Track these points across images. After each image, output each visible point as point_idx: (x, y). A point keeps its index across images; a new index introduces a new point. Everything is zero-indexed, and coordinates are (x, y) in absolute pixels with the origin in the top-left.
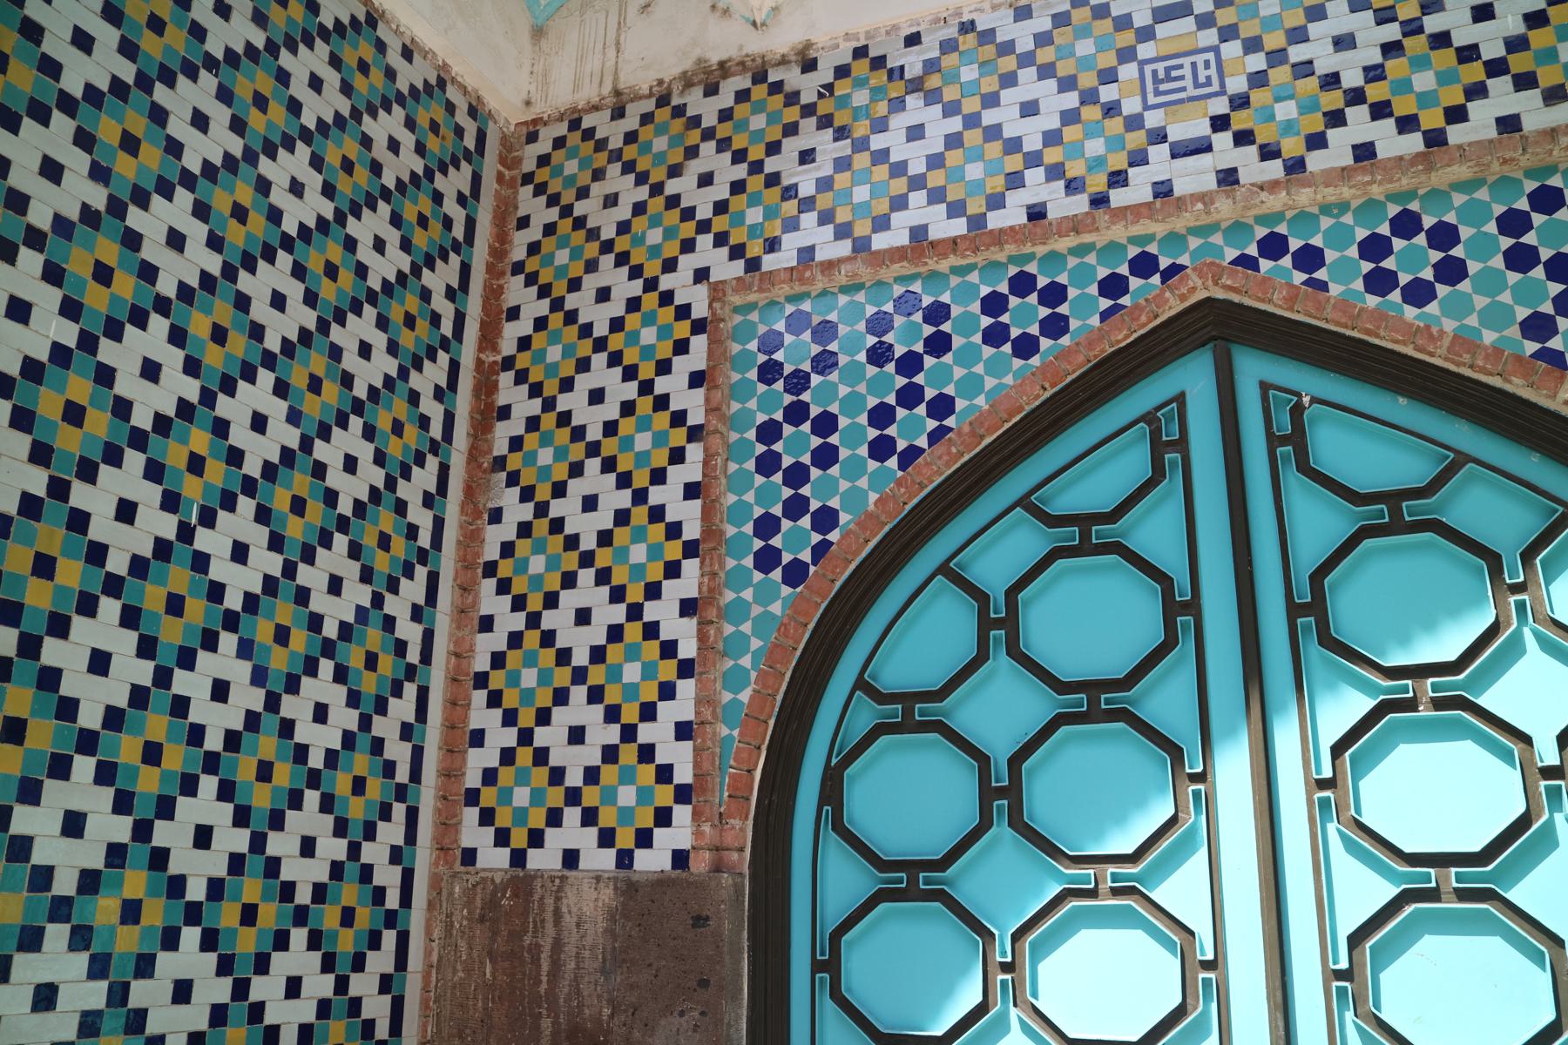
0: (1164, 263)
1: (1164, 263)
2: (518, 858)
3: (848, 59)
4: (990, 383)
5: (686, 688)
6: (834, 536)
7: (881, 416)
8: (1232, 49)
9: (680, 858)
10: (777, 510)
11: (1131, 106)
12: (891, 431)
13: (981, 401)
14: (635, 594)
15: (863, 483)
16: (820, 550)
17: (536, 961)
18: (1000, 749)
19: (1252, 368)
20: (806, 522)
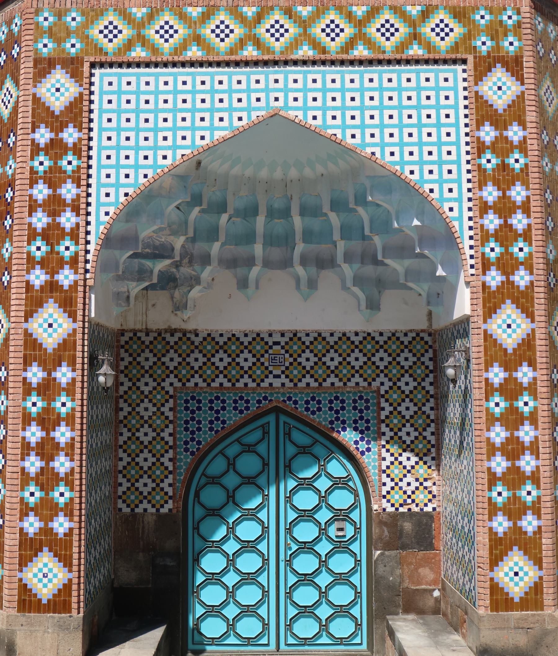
0: (269, 398)
1: (269, 398)
3: (206, 336)
4: (234, 418)
5: (171, 476)
7: (211, 422)
8: (287, 356)
10: (189, 440)
11: (266, 364)
12: (213, 426)
13: (232, 422)
14: (158, 456)
15: (207, 436)
16: (198, 449)
19: (283, 418)
20: (195, 443)
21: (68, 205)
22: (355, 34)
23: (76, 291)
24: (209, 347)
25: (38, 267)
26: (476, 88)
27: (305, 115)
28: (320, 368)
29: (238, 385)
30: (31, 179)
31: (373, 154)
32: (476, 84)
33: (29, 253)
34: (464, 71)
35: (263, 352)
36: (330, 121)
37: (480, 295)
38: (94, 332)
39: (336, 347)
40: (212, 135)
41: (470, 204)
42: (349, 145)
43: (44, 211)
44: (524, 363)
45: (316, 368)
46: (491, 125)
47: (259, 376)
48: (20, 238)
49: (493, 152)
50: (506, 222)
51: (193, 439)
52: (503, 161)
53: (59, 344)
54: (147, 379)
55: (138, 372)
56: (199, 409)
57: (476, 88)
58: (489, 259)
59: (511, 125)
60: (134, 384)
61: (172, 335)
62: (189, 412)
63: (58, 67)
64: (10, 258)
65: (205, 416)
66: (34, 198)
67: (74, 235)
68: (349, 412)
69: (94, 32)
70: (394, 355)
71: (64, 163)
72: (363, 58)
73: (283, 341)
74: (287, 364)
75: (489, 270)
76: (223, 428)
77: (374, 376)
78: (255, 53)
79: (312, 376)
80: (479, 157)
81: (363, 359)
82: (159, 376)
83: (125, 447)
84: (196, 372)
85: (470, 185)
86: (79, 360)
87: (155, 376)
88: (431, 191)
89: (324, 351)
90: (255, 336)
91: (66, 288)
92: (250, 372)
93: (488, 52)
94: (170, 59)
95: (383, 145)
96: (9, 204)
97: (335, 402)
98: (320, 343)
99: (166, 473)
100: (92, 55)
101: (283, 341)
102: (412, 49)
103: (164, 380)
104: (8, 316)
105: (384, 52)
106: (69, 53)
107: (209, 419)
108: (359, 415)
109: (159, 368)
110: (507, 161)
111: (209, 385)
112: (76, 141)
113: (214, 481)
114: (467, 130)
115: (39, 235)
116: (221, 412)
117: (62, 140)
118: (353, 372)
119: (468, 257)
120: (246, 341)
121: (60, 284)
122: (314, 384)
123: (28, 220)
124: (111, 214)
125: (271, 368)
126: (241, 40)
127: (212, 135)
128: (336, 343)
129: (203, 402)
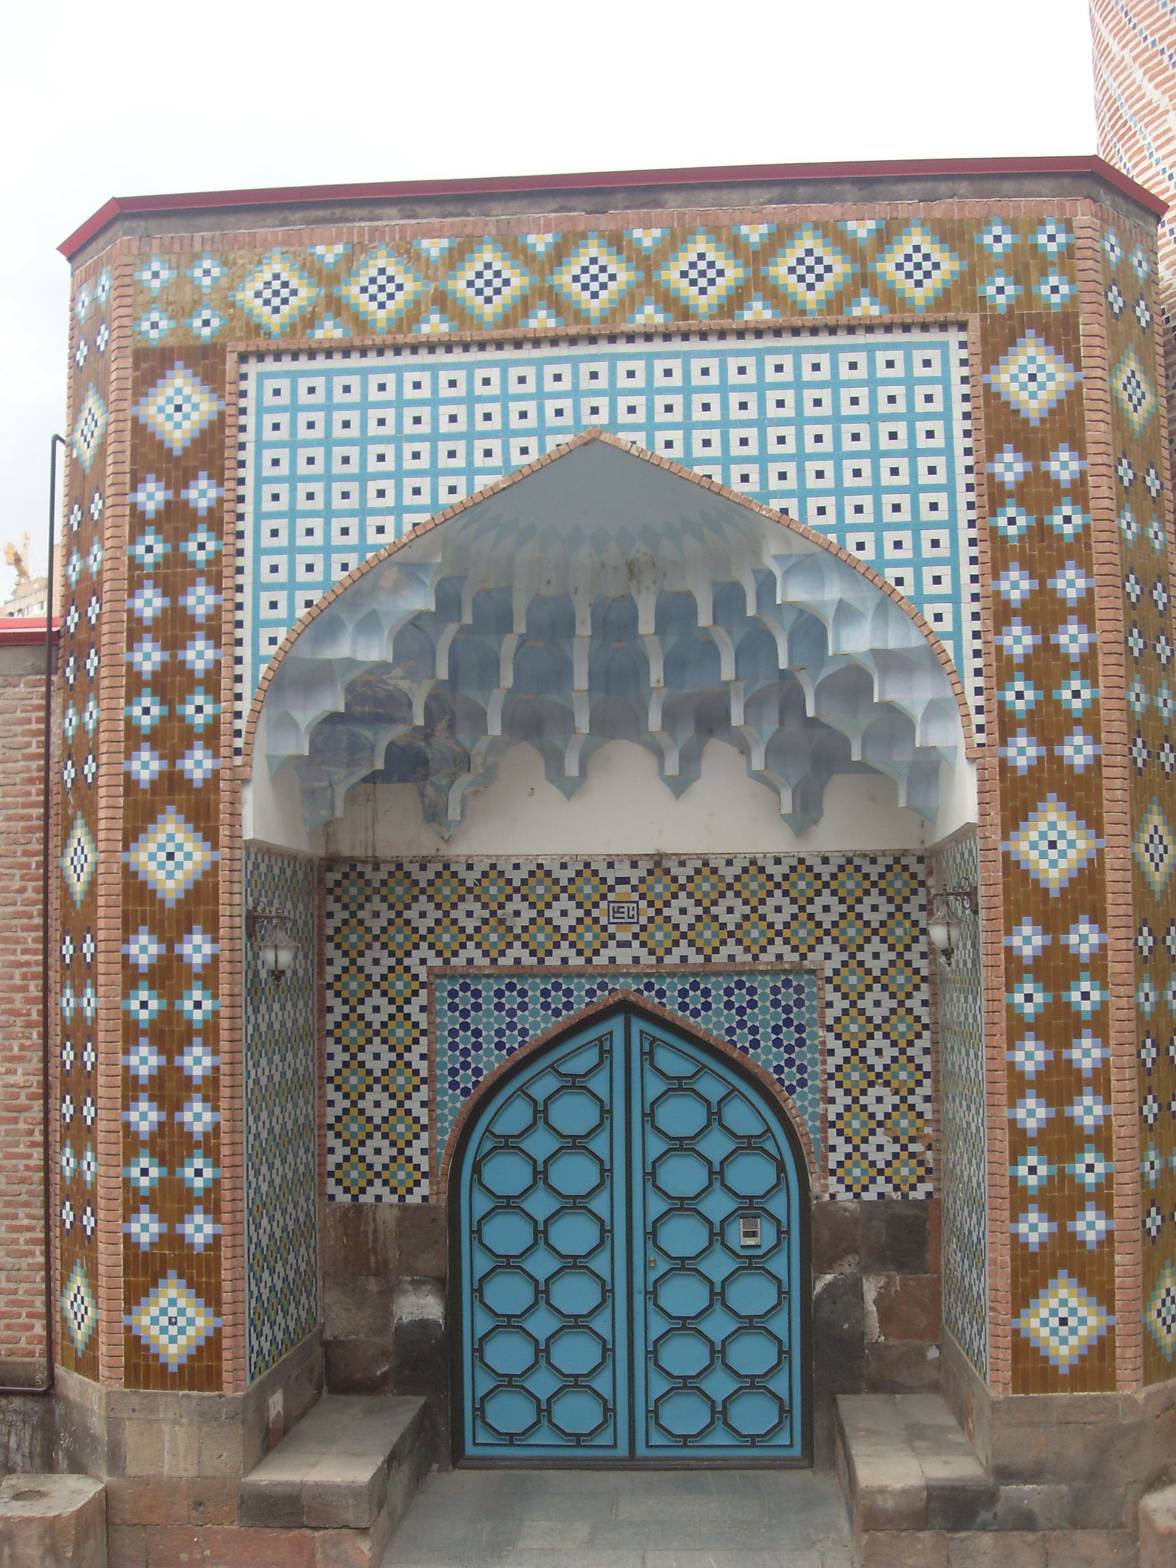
2: (355, 1198)
4: (543, 1025)
5: (425, 1135)
6: (481, 1079)
8: (643, 904)
9: (425, 1198)
10: (458, 1066)
16: (476, 1084)
17: (366, 1236)
18: (540, 1158)
19: (637, 1025)
20: (469, 1072)
21: (200, 627)
22: (747, 280)
23: (217, 790)
24: (493, 890)
25: (146, 745)
26: (985, 379)
27: (650, 441)
28: (707, 927)
29: (548, 961)
30: (131, 578)
31: (785, 511)
32: (986, 370)
33: (128, 720)
34: (963, 345)
35: (596, 898)
36: (698, 451)
37: (996, 784)
38: (256, 866)
39: (738, 886)
40: (470, 485)
41: (976, 607)
42: (736, 495)
43: (155, 640)
44: (1081, 917)
45: (699, 926)
46: (1016, 450)
47: (589, 944)
48: (113, 692)
49: (1020, 504)
50: (1046, 639)
51: (465, 1066)
52: (1040, 521)
53: (187, 892)
54: (376, 951)
55: (360, 938)
56: (477, 1007)
57: (985, 379)
58: (1013, 713)
59: (1056, 449)
60: (353, 962)
61: (423, 868)
62: (457, 1013)
63: (179, 364)
64: (96, 731)
65: (488, 1021)
66: (137, 615)
67: (211, 683)
68: (764, 1011)
69: (246, 296)
70: (850, 901)
71: (192, 546)
72: (762, 327)
73: (635, 876)
74: (643, 920)
75: (1014, 735)
76: (522, 1044)
77: (812, 941)
78: (551, 323)
79: (691, 943)
80: (993, 514)
81: (790, 909)
82: (400, 945)
83: (338, 1080)
84: (470, 938)
85: (975, 570)
86: (224, 921)
87: (392, 946)
88: (899, 581)
89: (714, 895)
90: (581, 867)
91: (198, 784)
92: (572, 937)
93: (1010, 308)
94: (389, 340)
95: (802, 494)
96: (93, 628)
97: (736, 991)
98: (706, 880)
99: (416, 1128)
100: (241, 339)
101: (635, 876)
102: (859, 304)
103: (408, 954)
104: (95, 840)
105: (803, 312)
106: (199, 337)
107: (496, 1027)
108: (784, 1016)
109: (399, 931)
110: (1047, 520)
111: (494, 961)
112: (214, 504)
113: (509, 1144)
114: (970, 461)
115: (146, 684)
116: (519, 1013)
117: (186, 502)
118: (771, 933)
119: (972, 711)
120: (564, 876)
121: (186, 776)
122: (695, 959)
123: (125, 657)
124: (280, 641)
125: (612, 929)
126: (524, 299)
127: (470, 485)
128: (737, 878)
129: (484, 994)
